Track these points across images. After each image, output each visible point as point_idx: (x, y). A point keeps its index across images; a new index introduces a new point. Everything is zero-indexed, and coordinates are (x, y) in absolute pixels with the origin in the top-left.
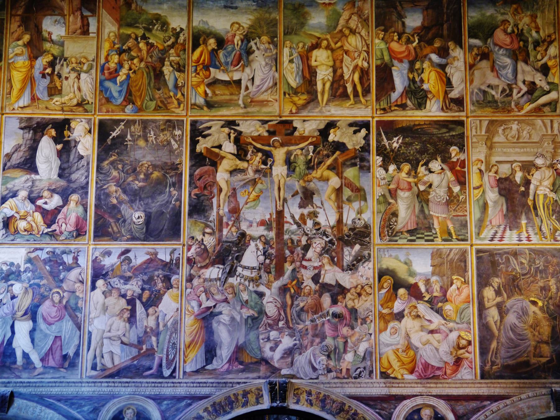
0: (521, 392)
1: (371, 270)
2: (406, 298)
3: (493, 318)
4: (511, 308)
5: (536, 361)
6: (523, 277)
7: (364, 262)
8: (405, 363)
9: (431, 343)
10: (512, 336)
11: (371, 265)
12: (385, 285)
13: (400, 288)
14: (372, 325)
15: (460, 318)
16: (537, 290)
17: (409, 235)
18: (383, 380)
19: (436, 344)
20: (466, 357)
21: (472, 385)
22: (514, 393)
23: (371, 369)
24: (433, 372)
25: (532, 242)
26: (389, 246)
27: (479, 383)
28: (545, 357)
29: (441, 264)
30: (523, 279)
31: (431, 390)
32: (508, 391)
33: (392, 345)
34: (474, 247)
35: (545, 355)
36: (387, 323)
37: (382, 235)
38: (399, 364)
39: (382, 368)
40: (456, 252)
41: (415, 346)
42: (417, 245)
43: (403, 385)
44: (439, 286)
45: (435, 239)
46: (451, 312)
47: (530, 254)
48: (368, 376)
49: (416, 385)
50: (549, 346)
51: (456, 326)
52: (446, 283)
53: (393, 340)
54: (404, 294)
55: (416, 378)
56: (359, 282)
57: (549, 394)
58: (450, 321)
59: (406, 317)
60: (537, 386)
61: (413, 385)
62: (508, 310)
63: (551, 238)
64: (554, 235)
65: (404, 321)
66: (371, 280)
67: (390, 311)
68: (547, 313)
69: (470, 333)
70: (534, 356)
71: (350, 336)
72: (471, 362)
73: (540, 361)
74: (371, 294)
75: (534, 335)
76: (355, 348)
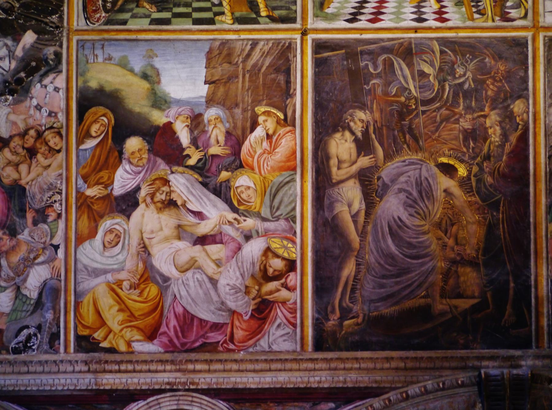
0: (409, 379)
1: (62, 94)
2: (145, 161)
3: (350, 206)
4: (393, 181)
5: (447, 308)
6: (424, 108)
7: (46, 74)
8: (136, 314)
9: (199, 268)
10: (393, 248)
11: (60, 81)
12: (94, 129)
13: (129, 136)
14: (61, 224)
15: (271, 207)
16: (456, 138)
17: (154, 9)
18: (82, 356)
19: (211, 268)
20: (280, 300)
21: (295, 366)
22: (393, 382)
23: (54, 330)
24: (203, 336)
25: (449, 24)
26: (106, 36)
27: (312, 360)
28: (468, 297)
29: (231, 78)
30: (424, 112)
31: (196, 378)
32: (378, 378)
33: (105, 272)
34: (310, 38)
35: (469, 293)
36: (95, 221)
37: (90, 8)
38: (121, 317)
39: (80, 328)
40: (266, 48)
41: (162, 275)
42: (174, 31)
43: (130, 367)
44: (224, 130)
45: (217, 18)
46: (250, 192)
47: (442, 52)
48: (46, 347)
49: (160, 368)
50: (478, 271)
51: (260, 225)
52: (239, 124)
53: (110, 261)
54: (140, 150)
55: (161, 350)
56: (31, 122)
57: (473, 385)
58: (247, 213)
59: (142, 206)
60: (446, 364)
61: (153, 367)
62: (386, 187)
63: (494, 14)
64: (503, 6)
65: (136, 215)
66: (61, 117)
67: (105, 192)
68: (478, 193)
69: (294, 242)
70: (443, 295)
71: (7, 253)
72: (293, 311)
73: (456, 307)
74: (59, 151)
75: (444, 246)
76: (17, 280)
